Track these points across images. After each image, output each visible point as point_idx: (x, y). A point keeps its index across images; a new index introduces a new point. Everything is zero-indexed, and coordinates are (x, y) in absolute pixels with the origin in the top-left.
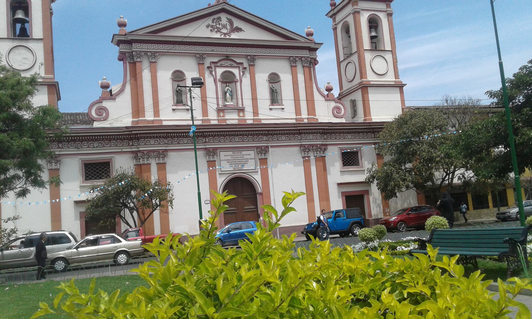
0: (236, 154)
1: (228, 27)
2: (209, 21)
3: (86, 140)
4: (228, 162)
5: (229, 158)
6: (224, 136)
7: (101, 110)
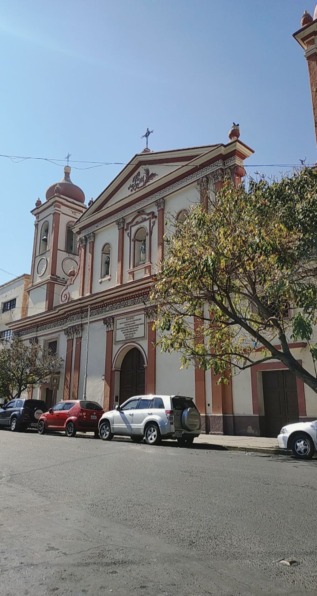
0: (129, 321)
1: (145, 178)
2: (130, 182)
3: (47, 324)
4: (122, 331)
5: (123, 326)
6: (119, 302)
7: (66, 296)
